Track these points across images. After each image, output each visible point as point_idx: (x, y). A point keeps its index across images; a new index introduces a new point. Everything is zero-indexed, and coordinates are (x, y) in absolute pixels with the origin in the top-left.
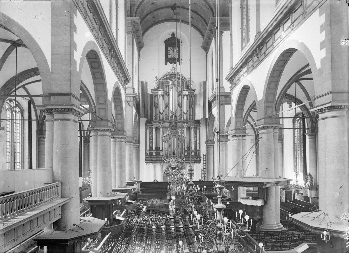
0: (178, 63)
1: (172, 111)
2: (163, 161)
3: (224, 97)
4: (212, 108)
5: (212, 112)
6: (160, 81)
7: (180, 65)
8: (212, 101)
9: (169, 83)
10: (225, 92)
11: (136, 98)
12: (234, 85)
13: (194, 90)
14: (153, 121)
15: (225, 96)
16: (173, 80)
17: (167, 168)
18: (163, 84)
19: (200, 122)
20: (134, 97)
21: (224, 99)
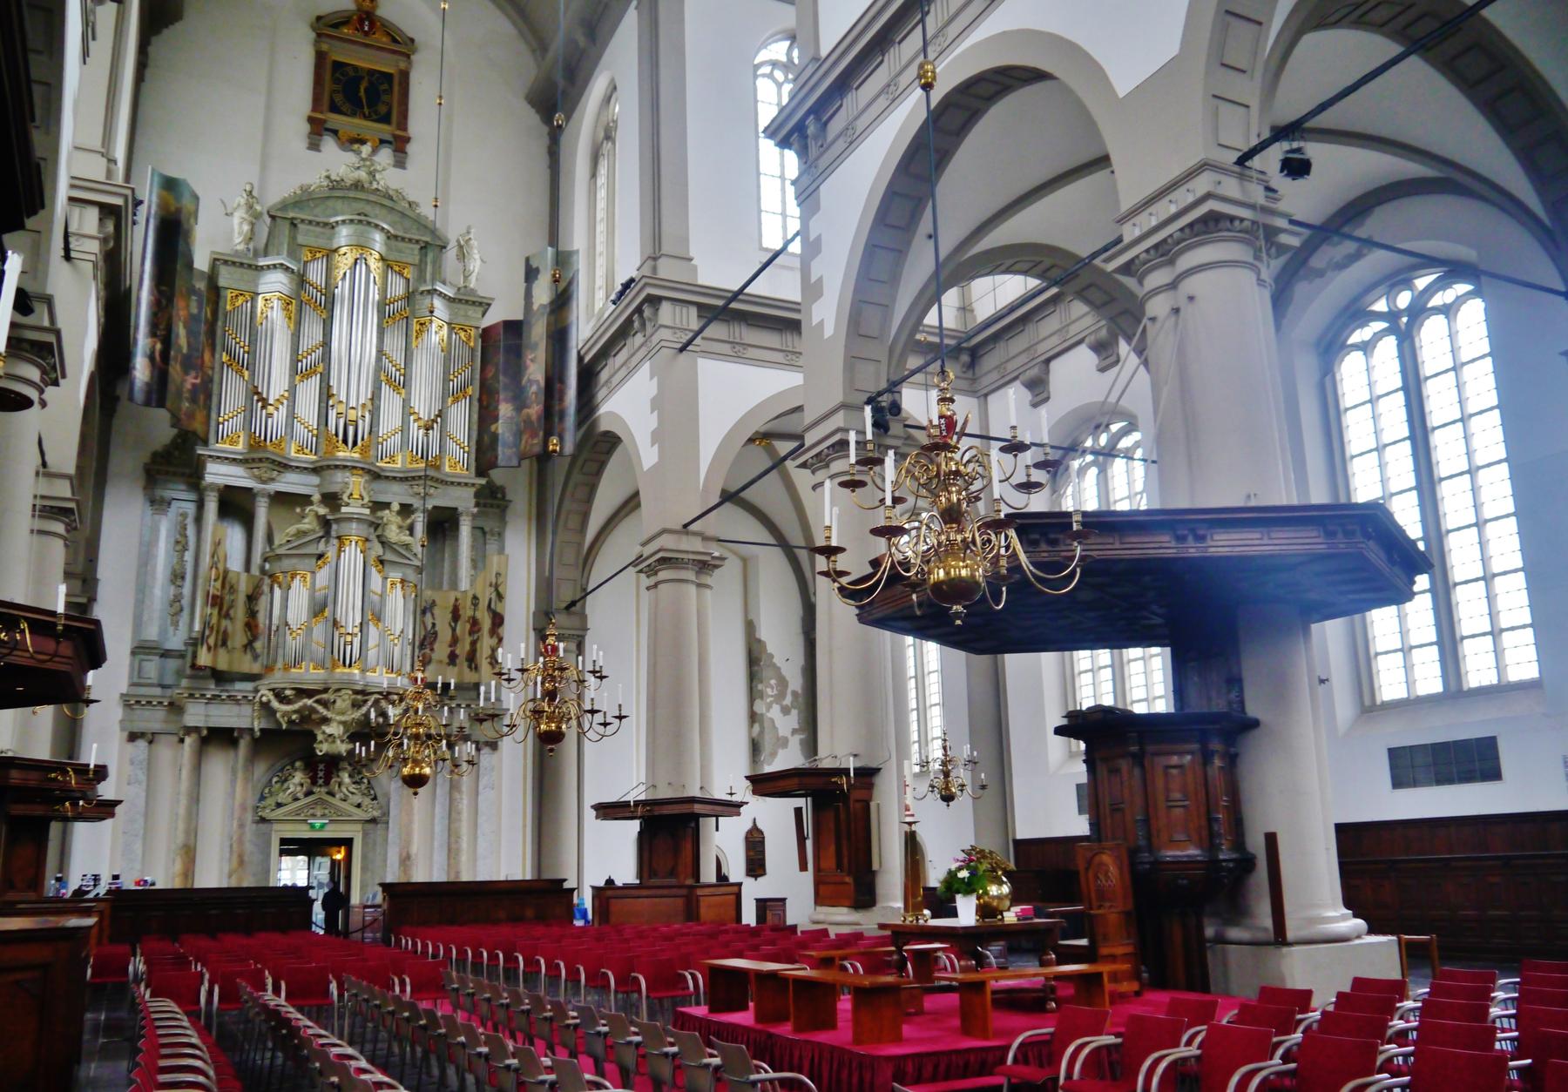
0: (385, 156)
1: (343, 398)
2: (265, 706)
3: (693, 311)
4: (601, 395)
5: (594, 425)
6: (273, 217)
7: (400, 164)
8: (605, 352)
9: (334, 234)
10: (700, 282)
11: (118, 227)
12: (840, 145)
13: (484, 305)
14: (206, 443)
15: (700, 306)
16: (360, 222)
17: (282, 770)
18: (293, 238)
19: (504, 496)
20: (107, 211)
21: (695, 324)
